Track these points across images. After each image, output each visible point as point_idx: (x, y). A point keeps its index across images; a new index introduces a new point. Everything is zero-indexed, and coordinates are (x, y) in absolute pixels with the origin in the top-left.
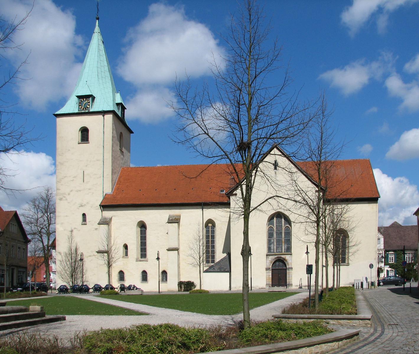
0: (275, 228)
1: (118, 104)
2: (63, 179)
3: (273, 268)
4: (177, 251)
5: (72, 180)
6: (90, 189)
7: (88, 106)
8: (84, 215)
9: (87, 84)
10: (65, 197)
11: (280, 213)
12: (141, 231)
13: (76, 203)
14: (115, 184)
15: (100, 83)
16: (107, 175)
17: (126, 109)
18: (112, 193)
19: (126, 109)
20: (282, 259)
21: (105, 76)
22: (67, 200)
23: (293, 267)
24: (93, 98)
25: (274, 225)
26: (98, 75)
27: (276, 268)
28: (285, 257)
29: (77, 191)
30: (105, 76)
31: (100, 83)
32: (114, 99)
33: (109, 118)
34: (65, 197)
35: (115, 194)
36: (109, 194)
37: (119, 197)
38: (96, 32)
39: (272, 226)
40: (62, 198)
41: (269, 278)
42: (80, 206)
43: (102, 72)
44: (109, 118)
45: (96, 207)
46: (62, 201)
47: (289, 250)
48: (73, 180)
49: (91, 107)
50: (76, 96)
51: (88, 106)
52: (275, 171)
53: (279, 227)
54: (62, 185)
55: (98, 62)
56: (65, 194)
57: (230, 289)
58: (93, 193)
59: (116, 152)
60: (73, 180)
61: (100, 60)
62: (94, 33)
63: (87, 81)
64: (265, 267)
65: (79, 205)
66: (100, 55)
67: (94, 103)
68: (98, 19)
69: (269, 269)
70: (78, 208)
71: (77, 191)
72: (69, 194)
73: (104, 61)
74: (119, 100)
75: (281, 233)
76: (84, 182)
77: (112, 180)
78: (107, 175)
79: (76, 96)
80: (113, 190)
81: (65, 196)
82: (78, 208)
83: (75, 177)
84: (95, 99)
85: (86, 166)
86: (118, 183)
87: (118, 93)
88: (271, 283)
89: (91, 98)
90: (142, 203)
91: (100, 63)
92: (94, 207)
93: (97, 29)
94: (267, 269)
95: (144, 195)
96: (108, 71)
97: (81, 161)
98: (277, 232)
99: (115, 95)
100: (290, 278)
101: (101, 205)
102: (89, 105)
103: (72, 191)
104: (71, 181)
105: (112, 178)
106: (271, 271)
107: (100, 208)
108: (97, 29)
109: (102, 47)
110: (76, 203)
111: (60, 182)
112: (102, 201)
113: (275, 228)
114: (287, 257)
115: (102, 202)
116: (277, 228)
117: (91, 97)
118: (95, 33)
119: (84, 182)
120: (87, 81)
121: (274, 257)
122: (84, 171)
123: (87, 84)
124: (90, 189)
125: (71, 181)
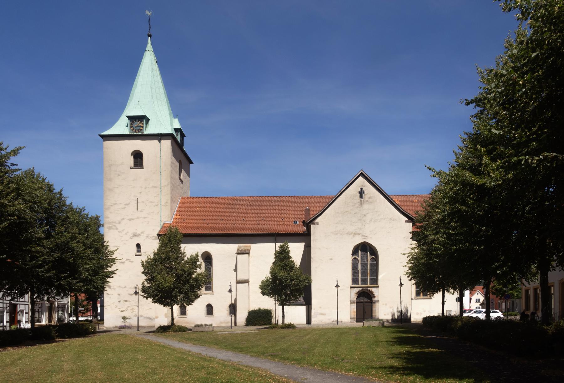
0: (359, 259)
1: (176, 130)
2: (112, 206)
3: (357, 301)
4: (248, 284)
5: (123, 207)
6: (145, 218)
7: (141, 128)
8: (138, 246)
9: (139, 104)
10: (114, 226)
11: (365, 244)
12: (205, 264)
13: (128, 232)
14: (175, 214)
15: (154, 105)
16: (166, 203)
17: (185, 137)
18: (172, 222)
19: (185, 137)
20: (367, 292)
21: (161, 98)
22: (117, 229)
23: (379, 300)
24: (148, 120)
25: (358, 257)
26: (152, 96)
27: (361, 301)
28: (372, 289)
29: (130, 220)
30: (161, 98)
31: (154, 105)
32: (172, 124)
33: (167, 144)
34: (114, 226)
35: (174, 223)
36: (167, 224)
37: (180, 226)
38: (149, 50)
39: (357, 257)
40: (111, 227)
41: (353, 311)
42: (133, 236)
43: (156, 93)
44: (167, 144)
45: (152, 237)
46: (111, 230)
47: (375, 281)
48: (125, 208)
49: (146, 130)
50: (126, 116)
51: (141, 128)
52: (360, 199)
53: (364, 259)
54: (111, 212)
55: (151, 82)
56: (115, 223)
57: (309, 321)
58: (149, 222)
59: (175, 179)
60: (125, 208)
61: (155, 81)
62: (146, 51)
63: (139, 101)
64: (349, 300)
65: (132, 234)
66: (154, 75)
67: (148, 125)
68: (150, 36)
69: (354, 302)
70: (130, 238)
71: (130, 220)
72: (120, 223)
73: (158, 83)
74: (178, 126)
75: (367, 264)
76: (137, 210)
77: (171, 209)
78: (166, 203)
79: (126, 116)
80: (173, 219)
81: (115, 224)
82: (130, 238)
83: (126, 205)
84: (150, 121)
85: (141, 193)
86: (178, 212)
87: (176, 118)
88: (355, 316)
89: (144, 121)
90: (208, 233)
91: (155, 83)
92: (150, 237)
93: (149, 47)
94: (351, 302)
95: (209, 224)
96: (164, 93)
97: (133, 187)
98: (362, 264)
99: (172, 120)
100: (377, 311)
101: (159, 234)
102: (143, 127)
103: (123, 219)
104: (123, 208)
105: (171, 207)
106: (355, 304)
107: (158, 238)
108: (149, 47)
109: (156, 67)
110: (128, 232)
111: (109, 210)
112: (160, 230)
113: (359, 259)
114: (374, 290)
115: (160, 232)
116: (362, 259)
117: (143, 119)
118: (147, 51)
119: (137, 210)
120: (139, 101)
121: (359, 289)
122: (137, 198)
123: (139, 104)
124: (145, 218)
125: (123, 208)
